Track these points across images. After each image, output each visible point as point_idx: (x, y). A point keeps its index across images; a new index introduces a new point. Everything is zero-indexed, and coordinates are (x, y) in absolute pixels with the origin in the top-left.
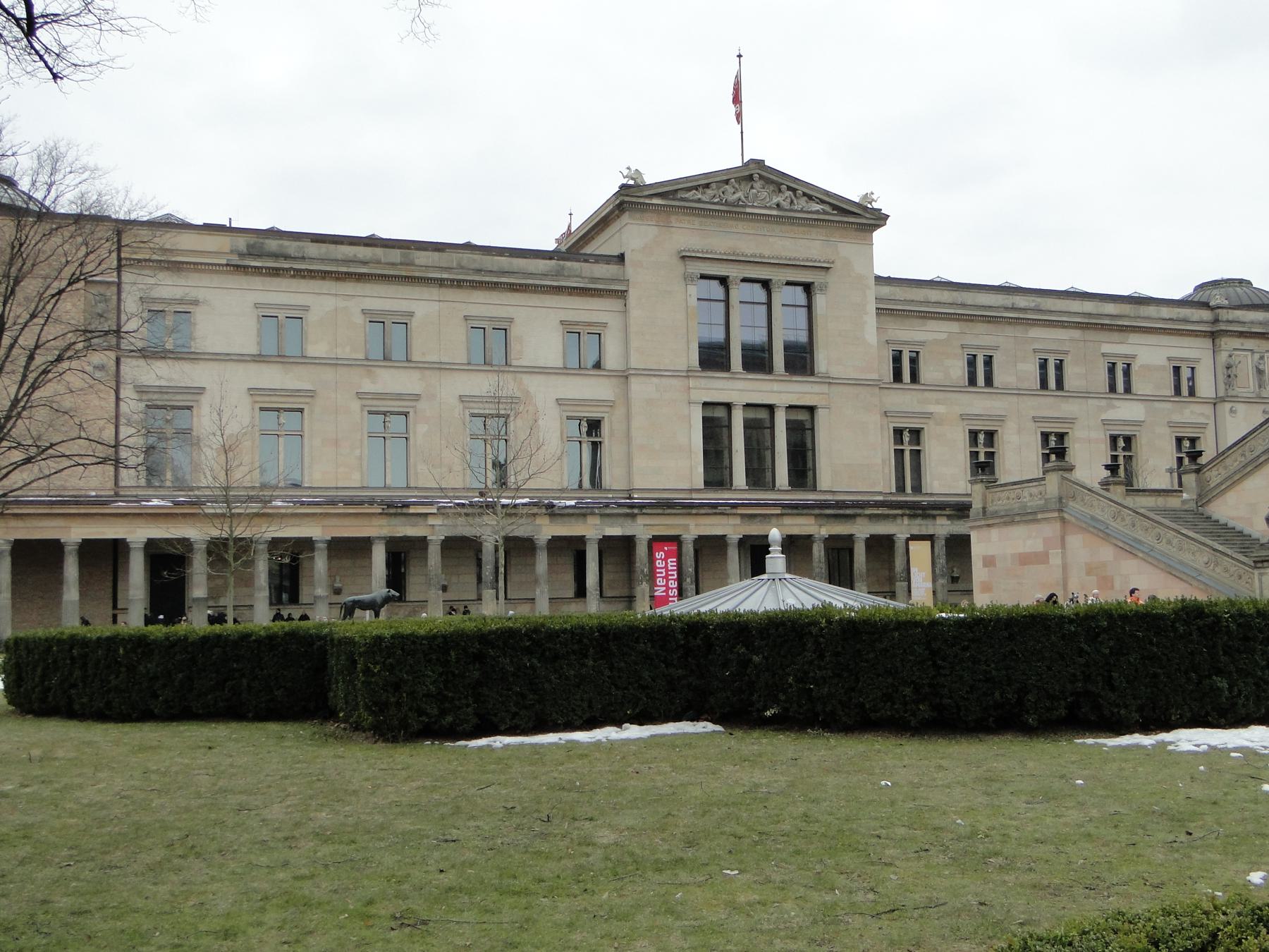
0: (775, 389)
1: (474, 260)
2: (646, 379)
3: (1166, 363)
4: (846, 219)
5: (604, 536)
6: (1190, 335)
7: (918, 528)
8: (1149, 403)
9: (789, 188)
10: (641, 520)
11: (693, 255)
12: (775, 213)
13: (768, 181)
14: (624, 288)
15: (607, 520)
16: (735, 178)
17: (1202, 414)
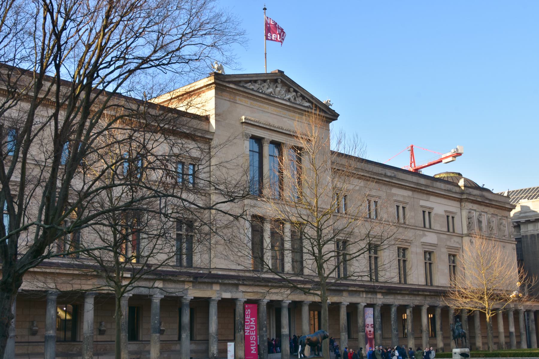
3: (443, 213)
6: (452, 200)
7: (369, 299)
8: (439, 234)
10: (241, 288)
11: (249, 122)
12: (288, 104)
13: (284, 84)
14: (211, 137)
15: (224, 288)
16: (269, 79)
17: (458, 242)
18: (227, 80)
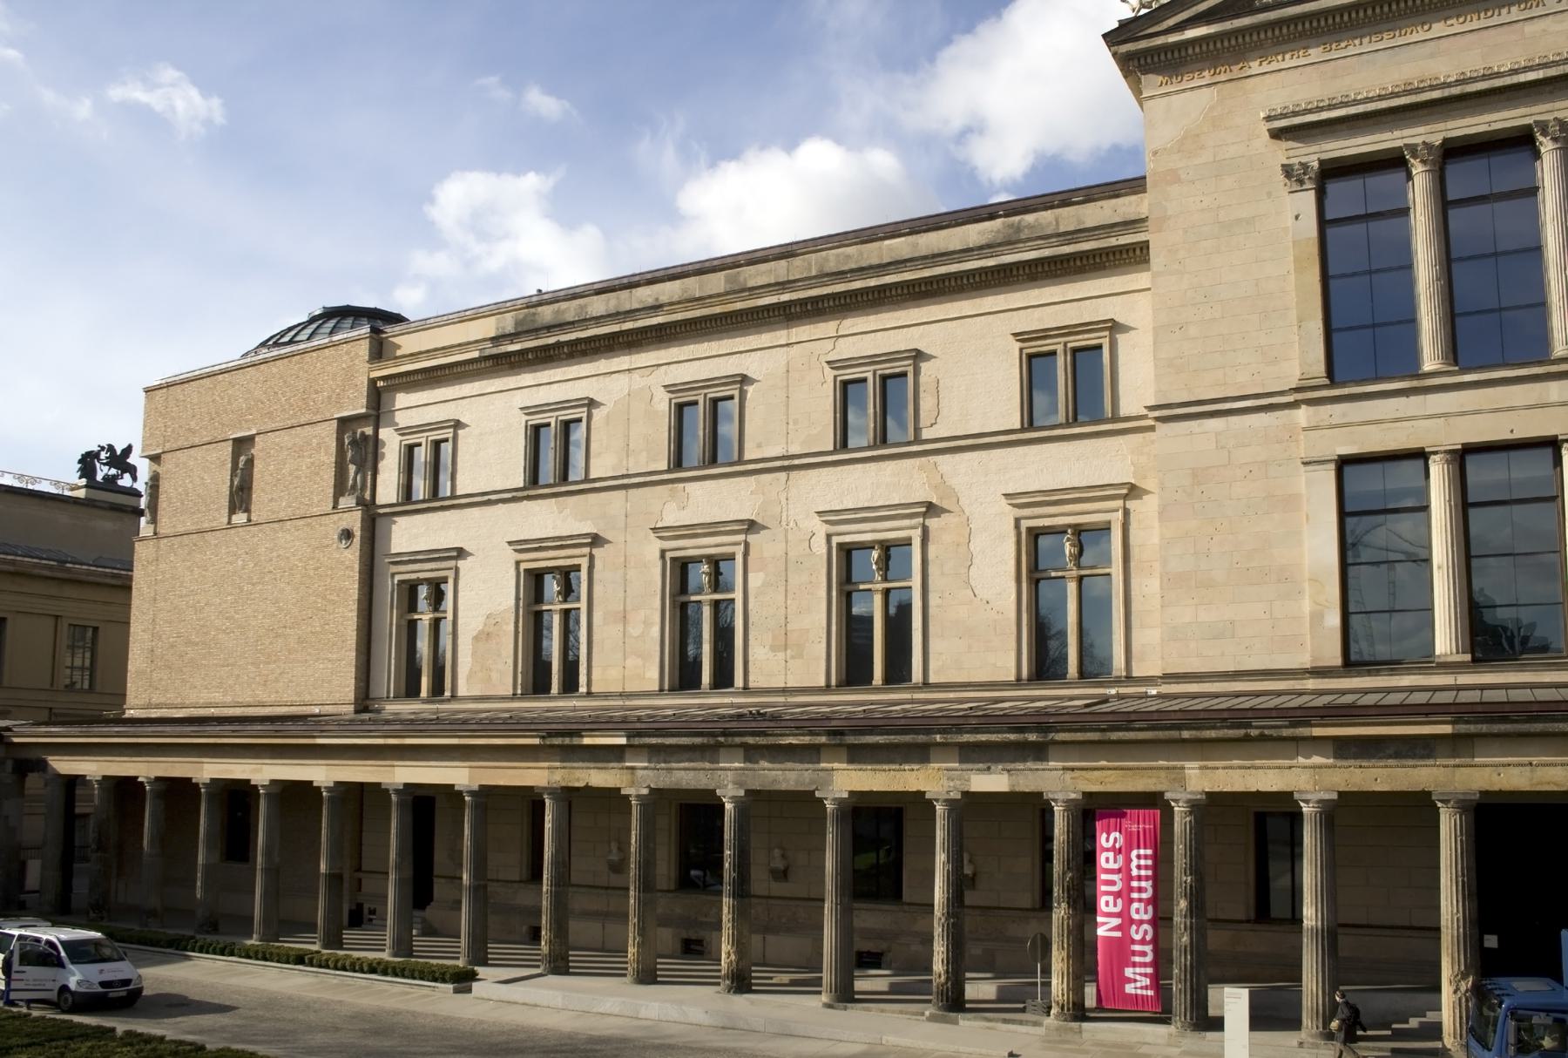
5: (966, 794)
18: (1171, 22)
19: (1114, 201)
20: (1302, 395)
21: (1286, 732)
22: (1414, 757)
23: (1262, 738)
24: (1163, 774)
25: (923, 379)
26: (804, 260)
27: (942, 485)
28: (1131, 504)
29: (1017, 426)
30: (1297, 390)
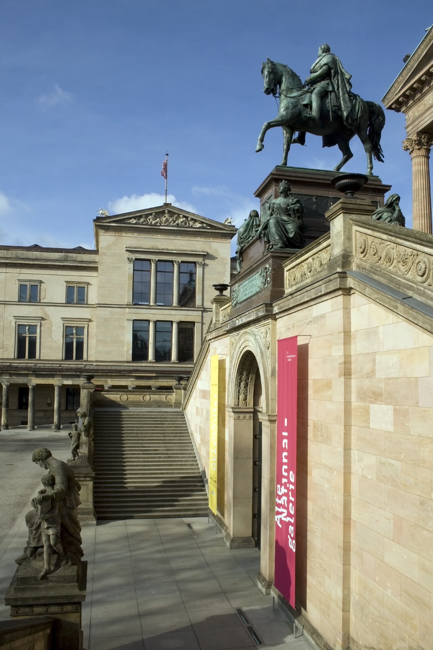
0: (173, 314)
1: (24, 254)
2: (105, 308)
4: (214, 231)
9: (184, 217)
12: (175, 228)
18: (108, 221)
19: (90, 255)
20: (128, 306)
21: (127, 374)
22: (149, 379)
23: (123, 375)
24: (104, 381)
25: (42, 288)
26: (11, 252)
27: (45, 314)
28: (89, 323)
29: (65, 302)
30: (127, 305)
